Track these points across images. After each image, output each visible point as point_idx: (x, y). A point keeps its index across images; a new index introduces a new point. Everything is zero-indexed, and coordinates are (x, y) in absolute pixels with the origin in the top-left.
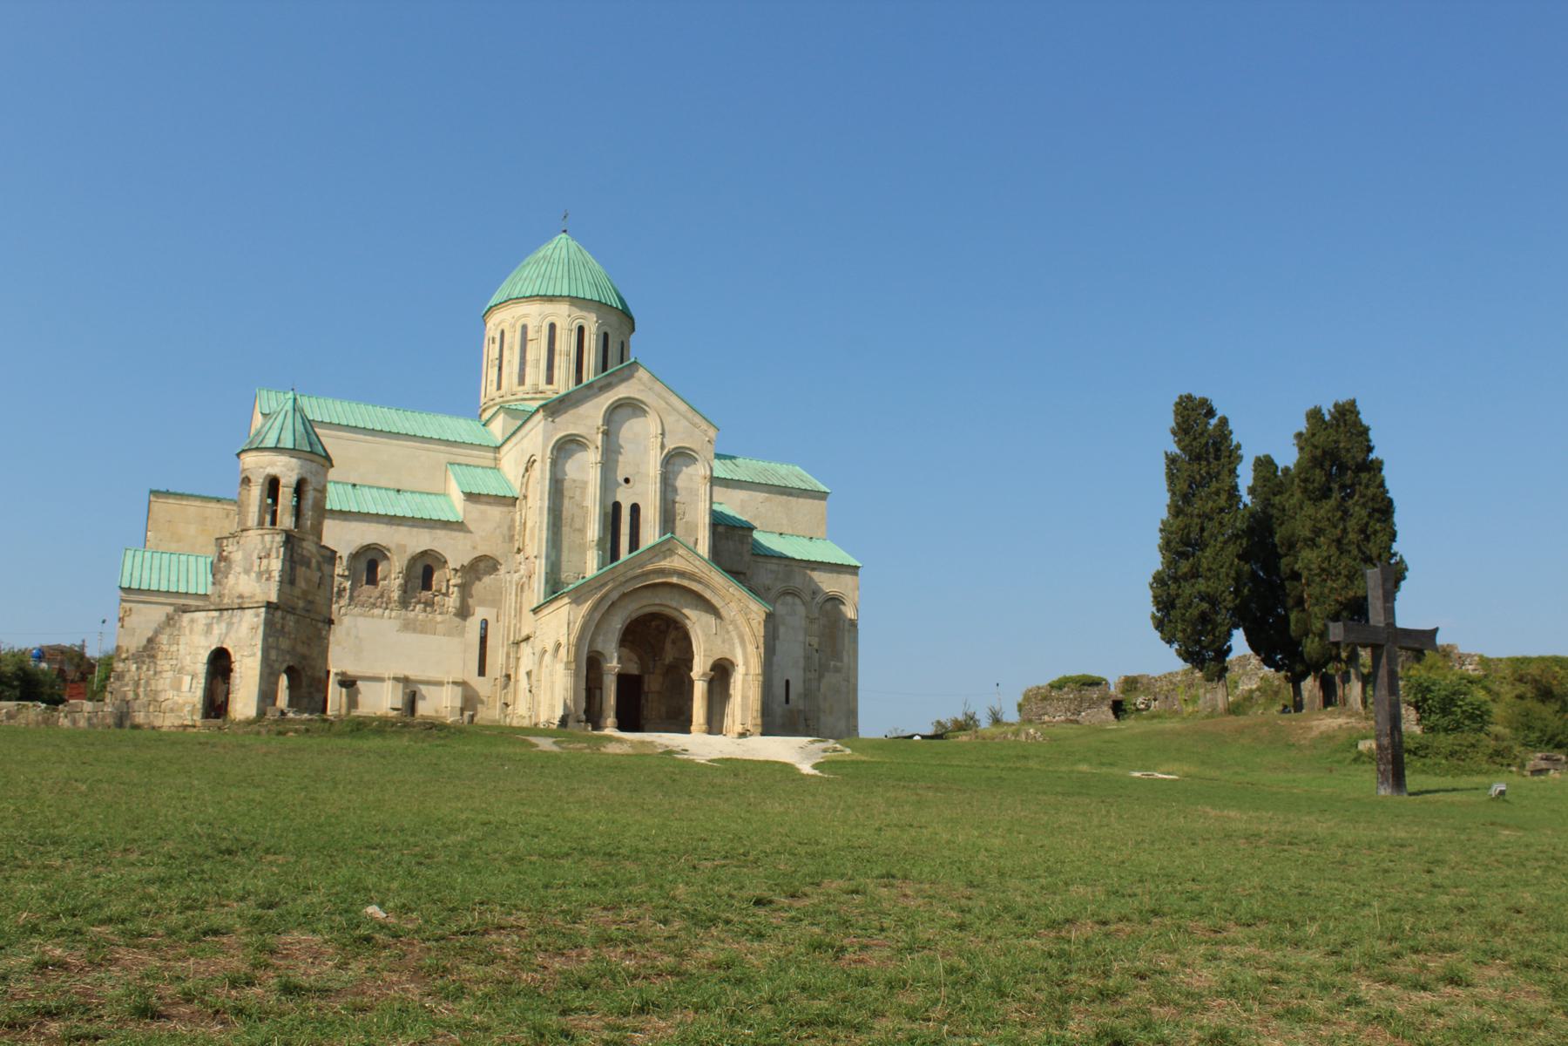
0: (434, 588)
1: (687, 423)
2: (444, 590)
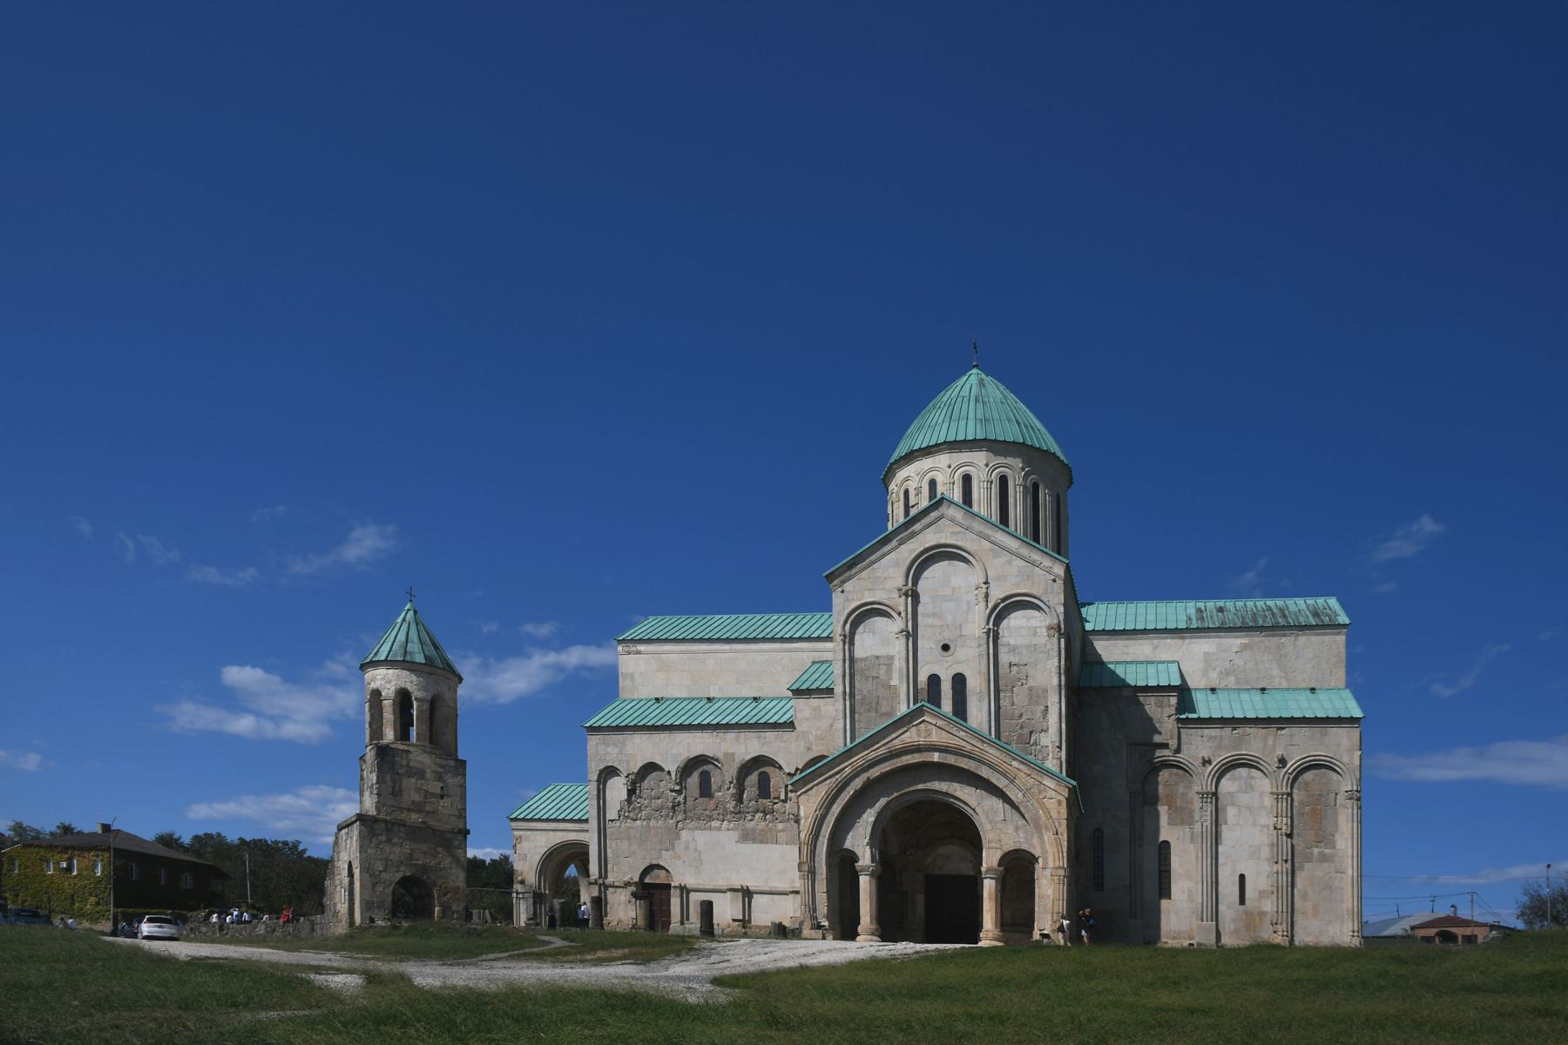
0: (772, 795)
1: (1023, 563)
2: (782, 797)
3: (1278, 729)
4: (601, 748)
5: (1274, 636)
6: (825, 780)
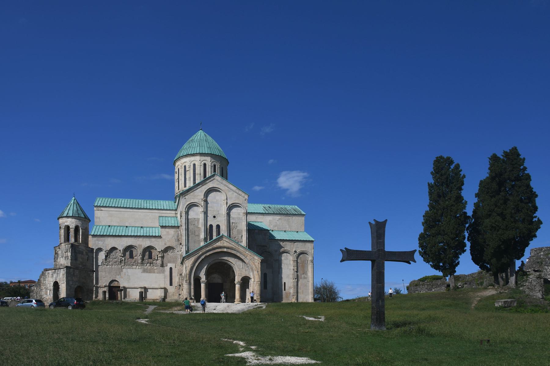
1: (237, 194)
2: (156, 259)
3: (294, 243)
4: (97, 242)
5: (287, 216)
6: (194, 256)
